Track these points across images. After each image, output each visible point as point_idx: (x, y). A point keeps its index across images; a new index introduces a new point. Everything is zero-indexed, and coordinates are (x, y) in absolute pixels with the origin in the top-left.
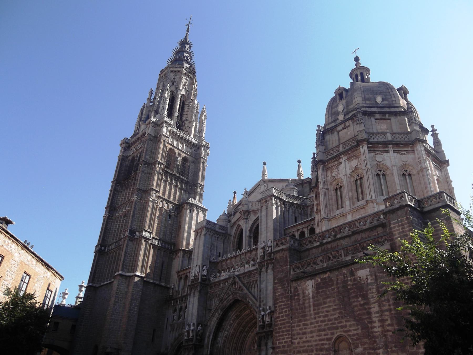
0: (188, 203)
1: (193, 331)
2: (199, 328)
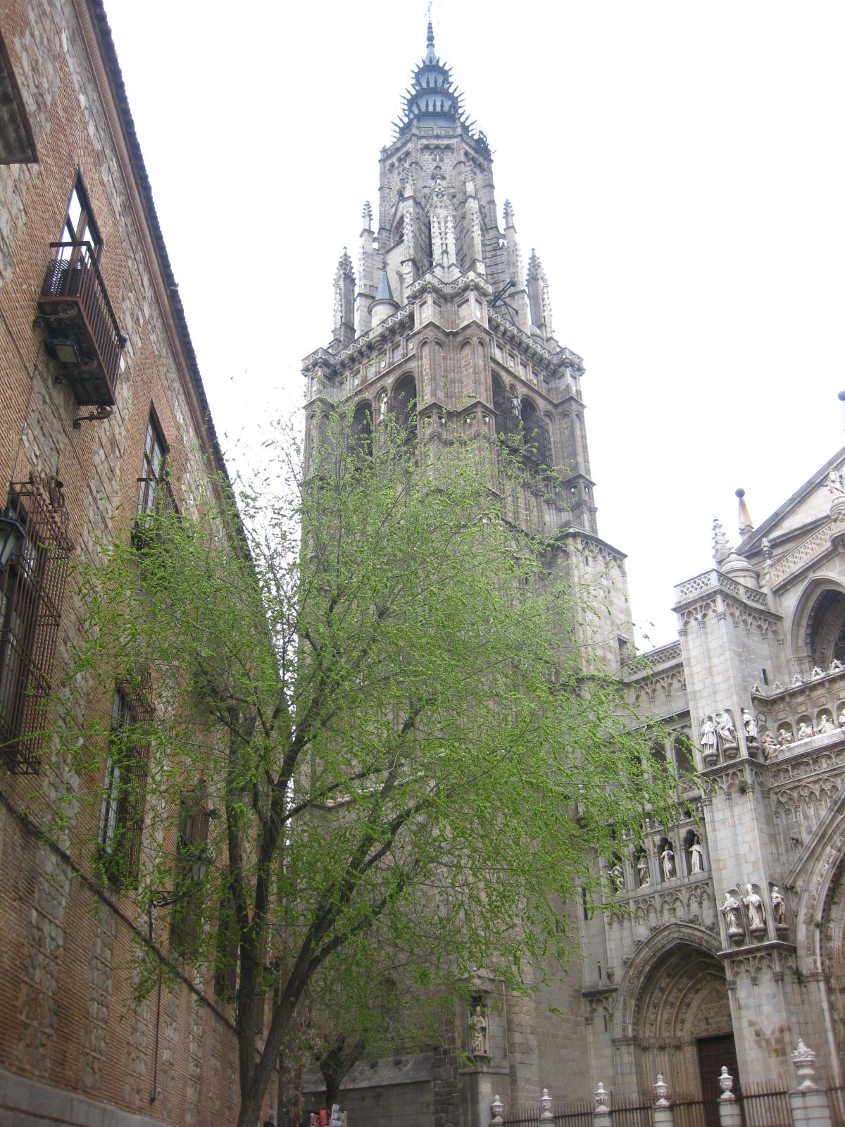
0: (574, 535)
1: (759, 907)
2: (777, 896)
